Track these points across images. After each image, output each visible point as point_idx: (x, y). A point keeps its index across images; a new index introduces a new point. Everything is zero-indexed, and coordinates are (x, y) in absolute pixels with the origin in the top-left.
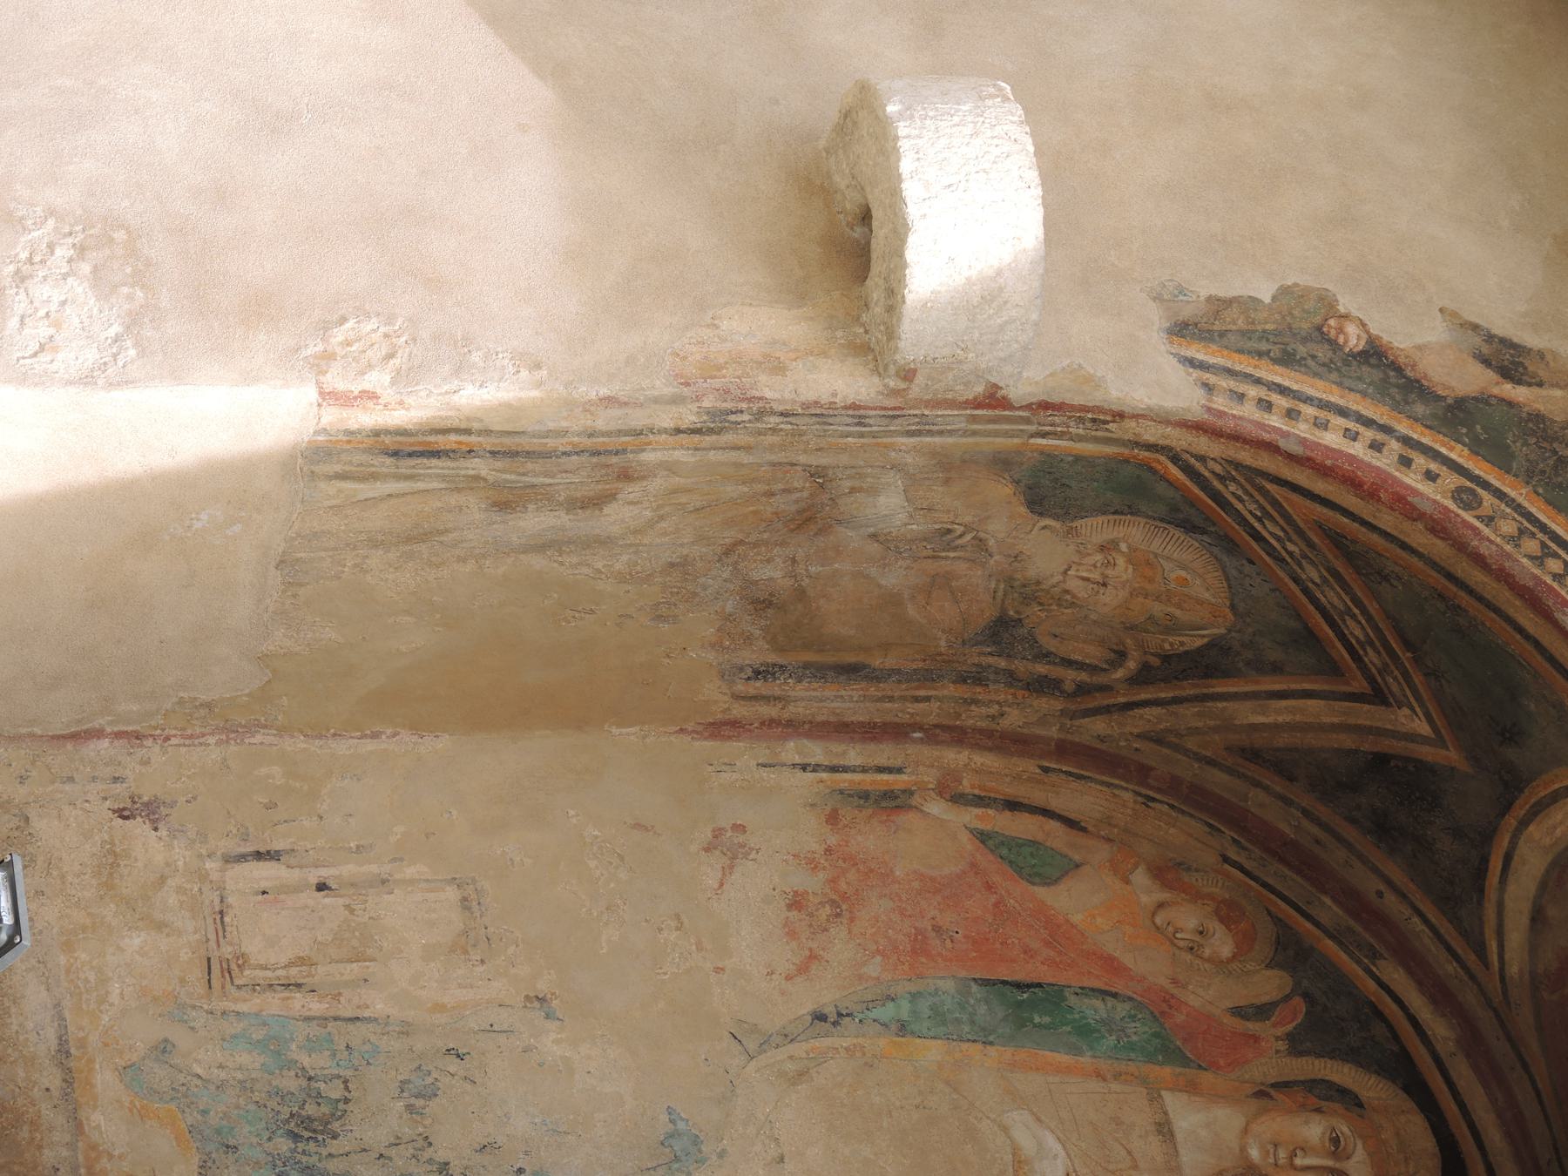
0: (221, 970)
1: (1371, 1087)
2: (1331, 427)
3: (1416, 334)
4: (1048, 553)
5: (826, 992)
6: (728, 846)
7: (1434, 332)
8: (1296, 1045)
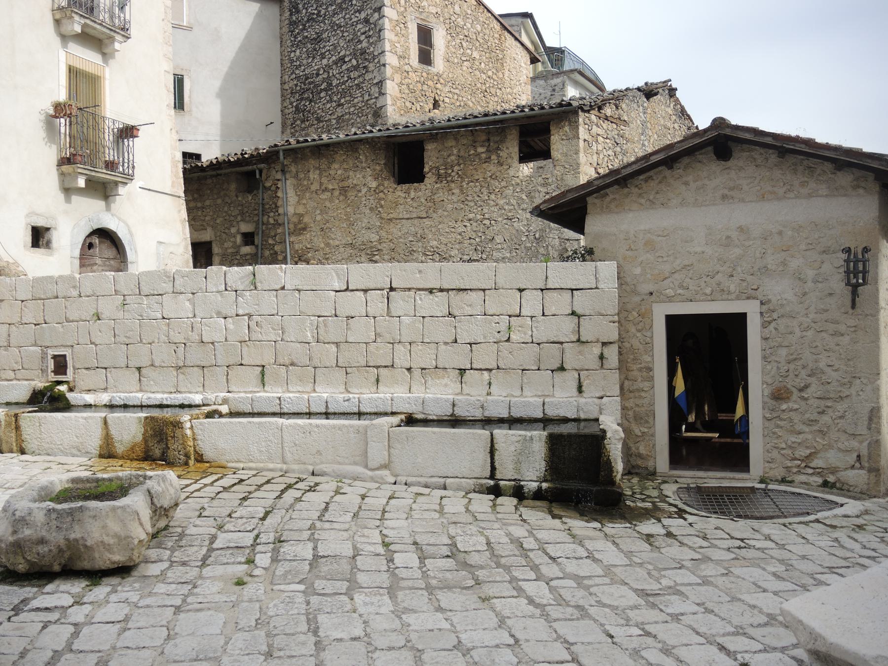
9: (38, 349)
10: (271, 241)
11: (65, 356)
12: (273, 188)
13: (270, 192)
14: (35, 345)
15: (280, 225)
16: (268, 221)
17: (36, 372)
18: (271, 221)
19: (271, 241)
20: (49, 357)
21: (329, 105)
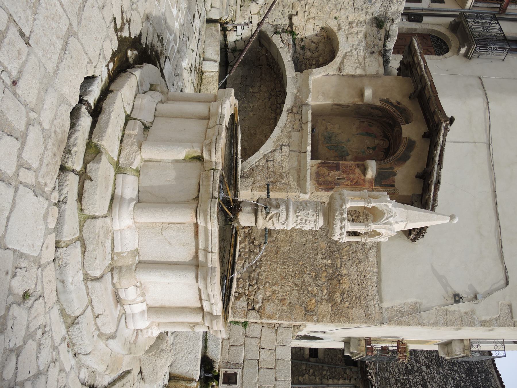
0: (326, 129)
1: (386, 140)
2: (387, 107)
3: (394, 101)
4: (372, 111)
5: (358, 133)
6: (354, 124)
7: (395, 101)
8: (383, 137)
9: (242, 362)
10: (311, 371)
11: (236, 383)
12: (345, 376)
13: (342, 373)
14: (245, 359)
15: (321, 380)
16: (324, 370)
17: (226, 358)
18: (324, 373)
19: (311, 371)
20: (236, 370)
21: (396, 370)
